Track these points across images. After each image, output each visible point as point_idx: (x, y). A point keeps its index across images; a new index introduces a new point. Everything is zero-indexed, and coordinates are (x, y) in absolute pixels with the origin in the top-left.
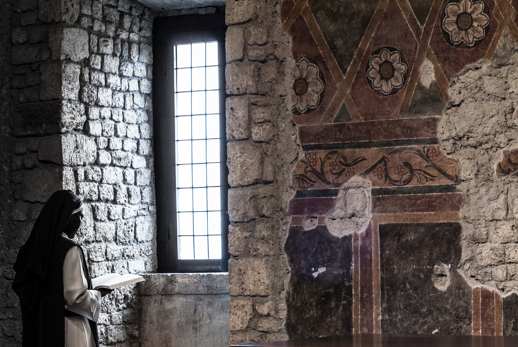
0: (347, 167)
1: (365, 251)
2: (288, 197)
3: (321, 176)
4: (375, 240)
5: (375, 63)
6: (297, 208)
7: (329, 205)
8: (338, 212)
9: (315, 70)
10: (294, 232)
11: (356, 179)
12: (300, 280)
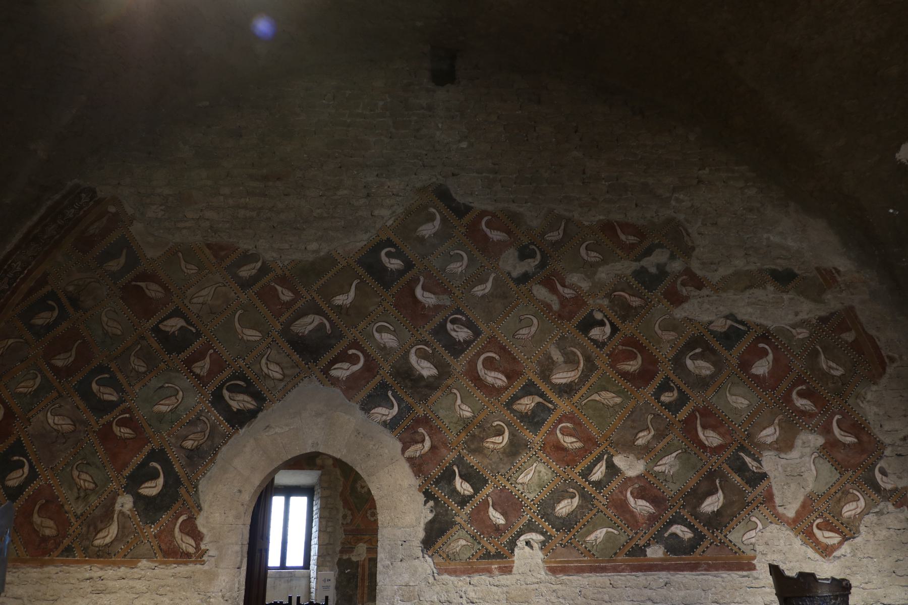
0: (359, 541)
1: (363, 565)
2: (338, 549)
3: (350, 543)
4: (367, 562)
5: (369, 512)
6: (341, 552)
7: (352, 552)
8: (354, 553)
9: (350, 512)
10: (340, 560)
11: (361, 544)
12: (341, 573)
